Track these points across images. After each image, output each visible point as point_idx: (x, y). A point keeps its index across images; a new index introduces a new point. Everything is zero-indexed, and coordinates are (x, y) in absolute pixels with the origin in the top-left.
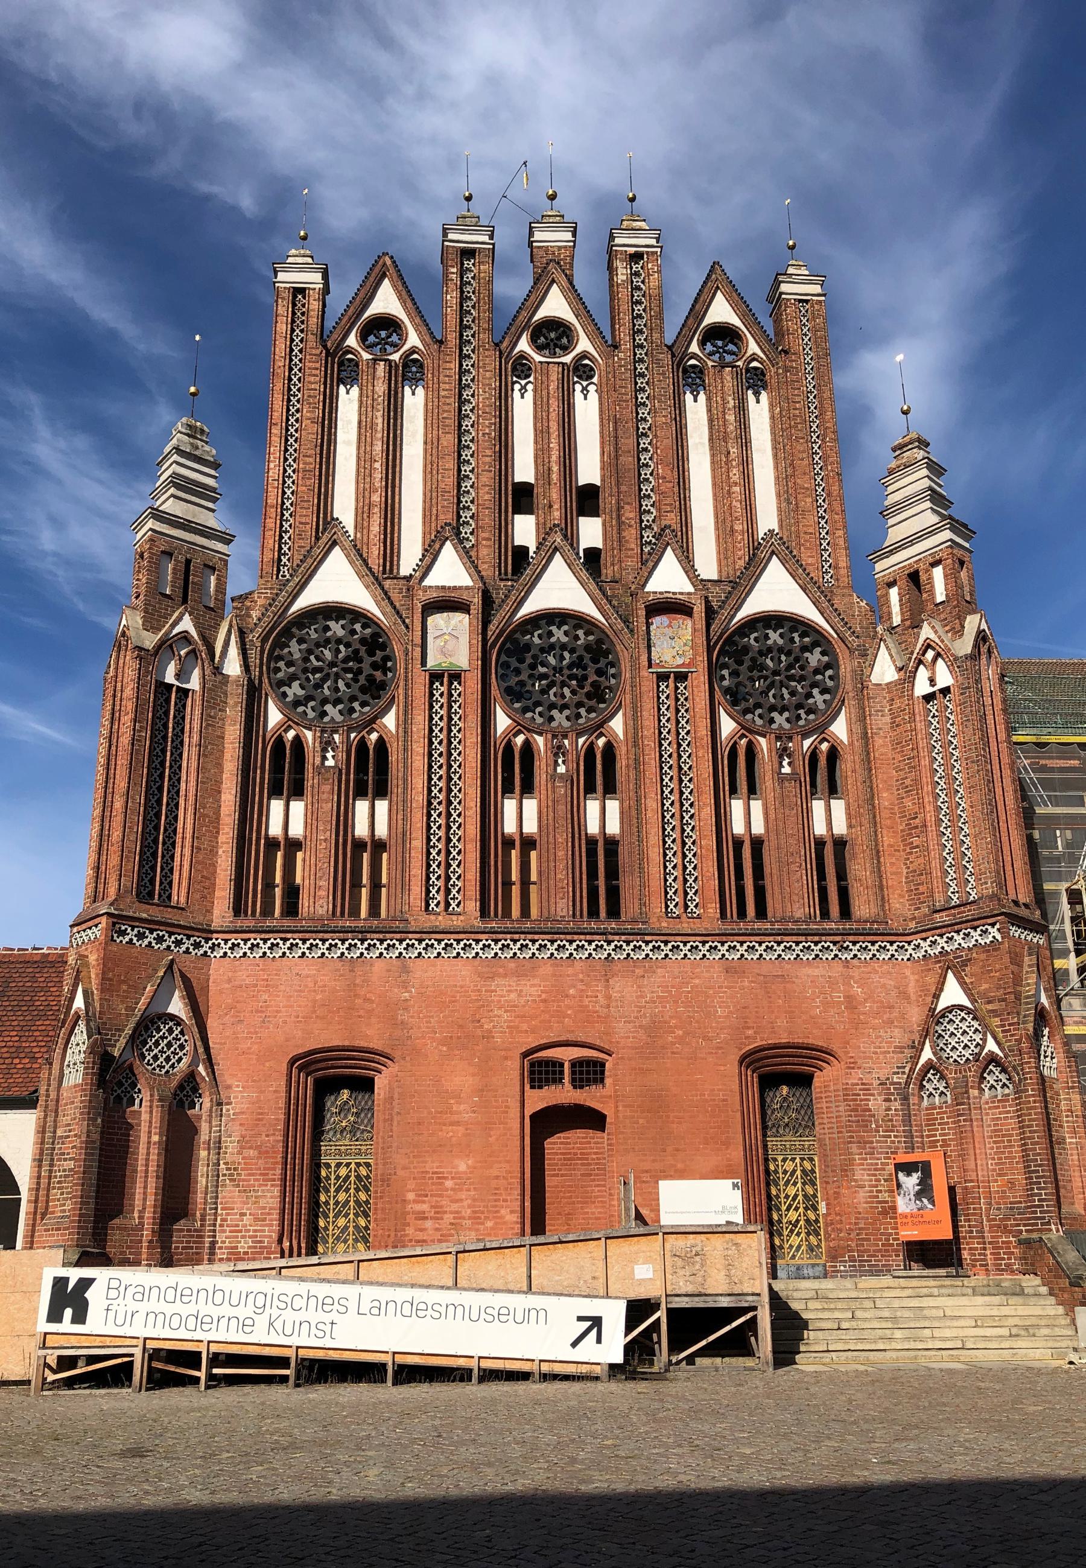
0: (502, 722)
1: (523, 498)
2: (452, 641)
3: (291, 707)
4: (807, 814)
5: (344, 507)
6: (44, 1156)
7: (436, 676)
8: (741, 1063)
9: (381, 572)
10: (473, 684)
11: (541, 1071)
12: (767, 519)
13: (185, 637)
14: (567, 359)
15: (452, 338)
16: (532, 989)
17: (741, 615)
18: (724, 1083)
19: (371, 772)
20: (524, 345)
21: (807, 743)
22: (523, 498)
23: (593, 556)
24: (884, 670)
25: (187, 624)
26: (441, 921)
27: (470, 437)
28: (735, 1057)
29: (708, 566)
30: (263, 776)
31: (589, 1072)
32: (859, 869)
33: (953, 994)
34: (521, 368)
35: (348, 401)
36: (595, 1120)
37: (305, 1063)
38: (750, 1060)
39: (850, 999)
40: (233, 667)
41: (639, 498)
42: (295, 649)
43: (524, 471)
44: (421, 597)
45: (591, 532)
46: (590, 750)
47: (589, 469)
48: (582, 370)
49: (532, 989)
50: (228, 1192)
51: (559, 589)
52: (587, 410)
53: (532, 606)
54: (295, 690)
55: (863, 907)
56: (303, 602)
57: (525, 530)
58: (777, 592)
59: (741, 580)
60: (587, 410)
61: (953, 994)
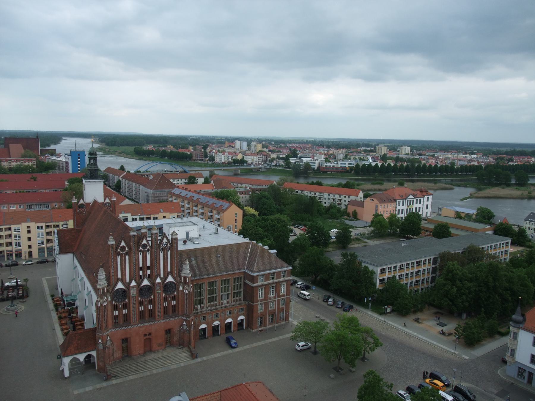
0: (139, 299)
1: (141, 269)
2: (133, 292)
3: (115, 301)
5: (119, 276)
6: (98, 354)
9: (124, 283)
11: (145, 335)
12: (169, 270)
16: (144, 328)
18: (163, 333)
19: (125, 306)
20: (141, 248)
22: (141, 269)
24: (181, 288)
27: (134, 262)
29: (162, 276)
31: (150, 334)
32: (177, 308)
33: (185, 323)
34: (141, 251)
35: (119, 259)
45: (149, 272)
47: (149, 264)
48: (148, 250)
49: (144, 328)
51: (146, 282)
52: (148, 256)
54: (115, 298)
55: (176, 312)
57: (141, 273)
58: (170, 279)
59: (166, 277)
60: (148, 256)
61: (185, 323)
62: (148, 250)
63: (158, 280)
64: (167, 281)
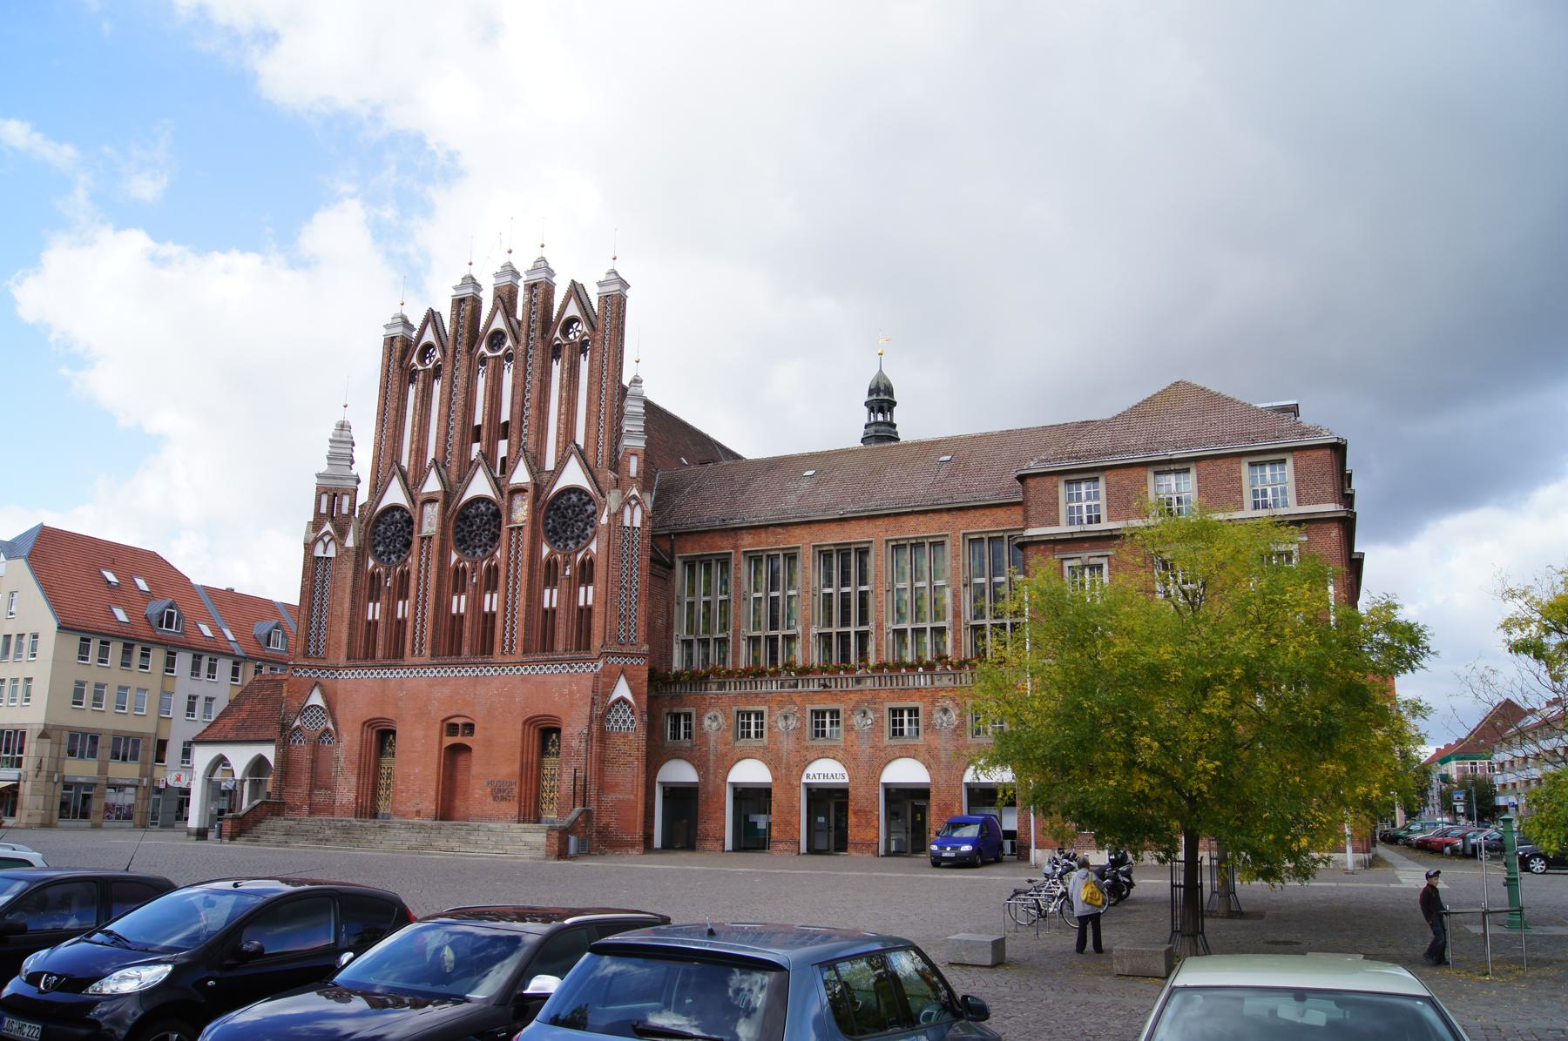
0: (454, 557)
1: (476, 434)
2: (430, 521)
3: (378, 557)
4: (576, 594)
7: (423, 539)
8: (525, 723)
10: (435, 544)
11: (452, 729)
13: (328, 533)
14: (500, 353)
15: (450, 352)
17: (555, 489)
20: (483, 348)
21: (579, 556)
22: (476, 434)
23: (504, 459)
25: (328, 527)
26: (416, 660)
28: (521, 721)
29: (550, 465)
30: (364, 593)
34: (483, 360)
36: (468, 749)
37: (369, 724)
38: (529, 722)
39: (571, 693)
40: (350, 542)
41: (521, 430)
42: (382, 527)
43: (478, 421)
44: (421, 498)
46: (489, 567)
47: (505, 416)
48: (509, 357)
49: (446, 691)
50: (340, 779)
51: (480, 486)
53: (468, 496)
54: (381, 549)
56: (383, 505)
58: (572, 475)
62: (509, 357)
63: (521, 476)
64: (563, 482)
